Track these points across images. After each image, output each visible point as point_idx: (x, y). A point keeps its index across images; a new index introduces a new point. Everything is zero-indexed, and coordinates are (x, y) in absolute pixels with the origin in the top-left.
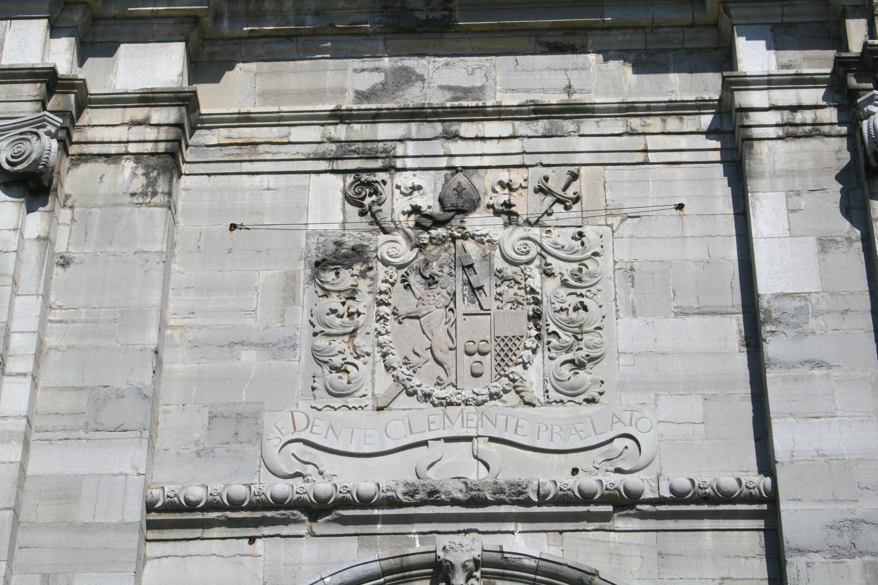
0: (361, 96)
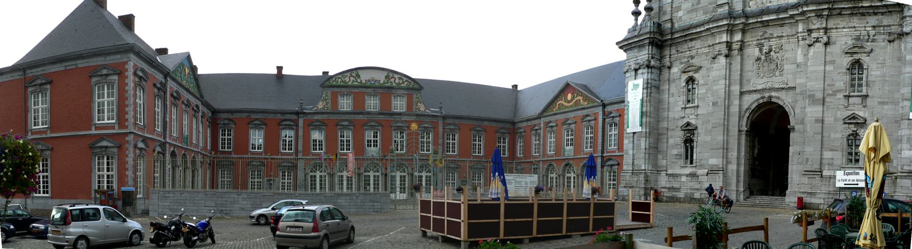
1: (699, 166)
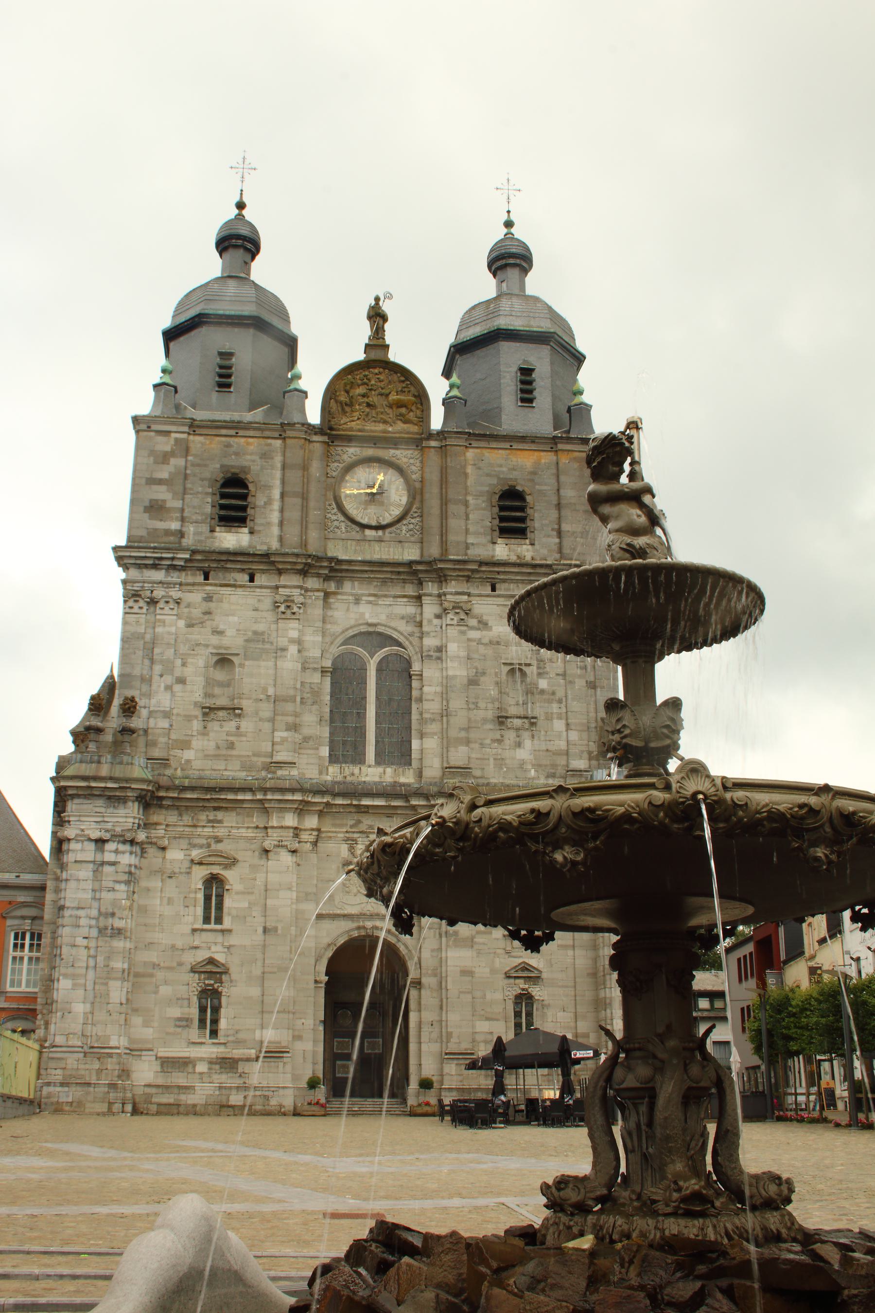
0: (351, 827)
1: (233, 1042)
